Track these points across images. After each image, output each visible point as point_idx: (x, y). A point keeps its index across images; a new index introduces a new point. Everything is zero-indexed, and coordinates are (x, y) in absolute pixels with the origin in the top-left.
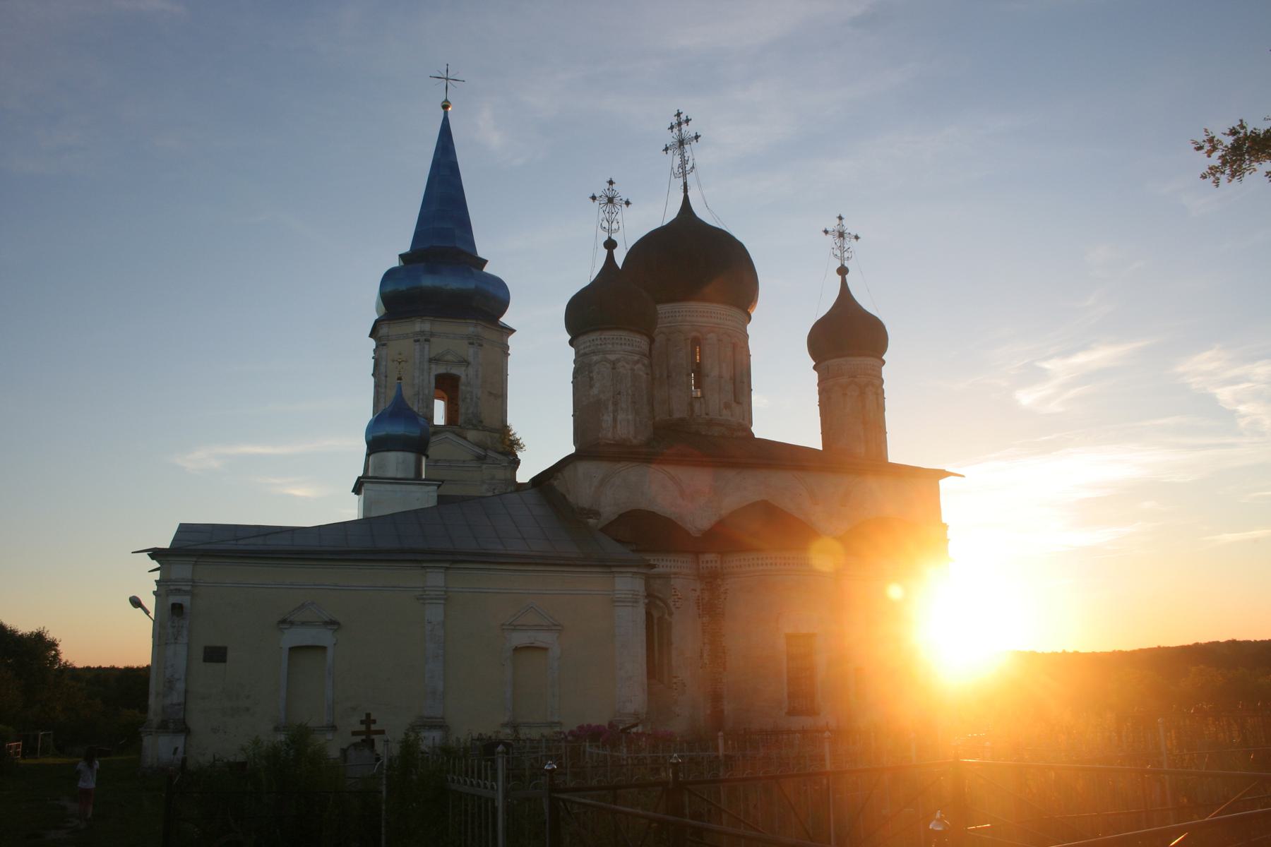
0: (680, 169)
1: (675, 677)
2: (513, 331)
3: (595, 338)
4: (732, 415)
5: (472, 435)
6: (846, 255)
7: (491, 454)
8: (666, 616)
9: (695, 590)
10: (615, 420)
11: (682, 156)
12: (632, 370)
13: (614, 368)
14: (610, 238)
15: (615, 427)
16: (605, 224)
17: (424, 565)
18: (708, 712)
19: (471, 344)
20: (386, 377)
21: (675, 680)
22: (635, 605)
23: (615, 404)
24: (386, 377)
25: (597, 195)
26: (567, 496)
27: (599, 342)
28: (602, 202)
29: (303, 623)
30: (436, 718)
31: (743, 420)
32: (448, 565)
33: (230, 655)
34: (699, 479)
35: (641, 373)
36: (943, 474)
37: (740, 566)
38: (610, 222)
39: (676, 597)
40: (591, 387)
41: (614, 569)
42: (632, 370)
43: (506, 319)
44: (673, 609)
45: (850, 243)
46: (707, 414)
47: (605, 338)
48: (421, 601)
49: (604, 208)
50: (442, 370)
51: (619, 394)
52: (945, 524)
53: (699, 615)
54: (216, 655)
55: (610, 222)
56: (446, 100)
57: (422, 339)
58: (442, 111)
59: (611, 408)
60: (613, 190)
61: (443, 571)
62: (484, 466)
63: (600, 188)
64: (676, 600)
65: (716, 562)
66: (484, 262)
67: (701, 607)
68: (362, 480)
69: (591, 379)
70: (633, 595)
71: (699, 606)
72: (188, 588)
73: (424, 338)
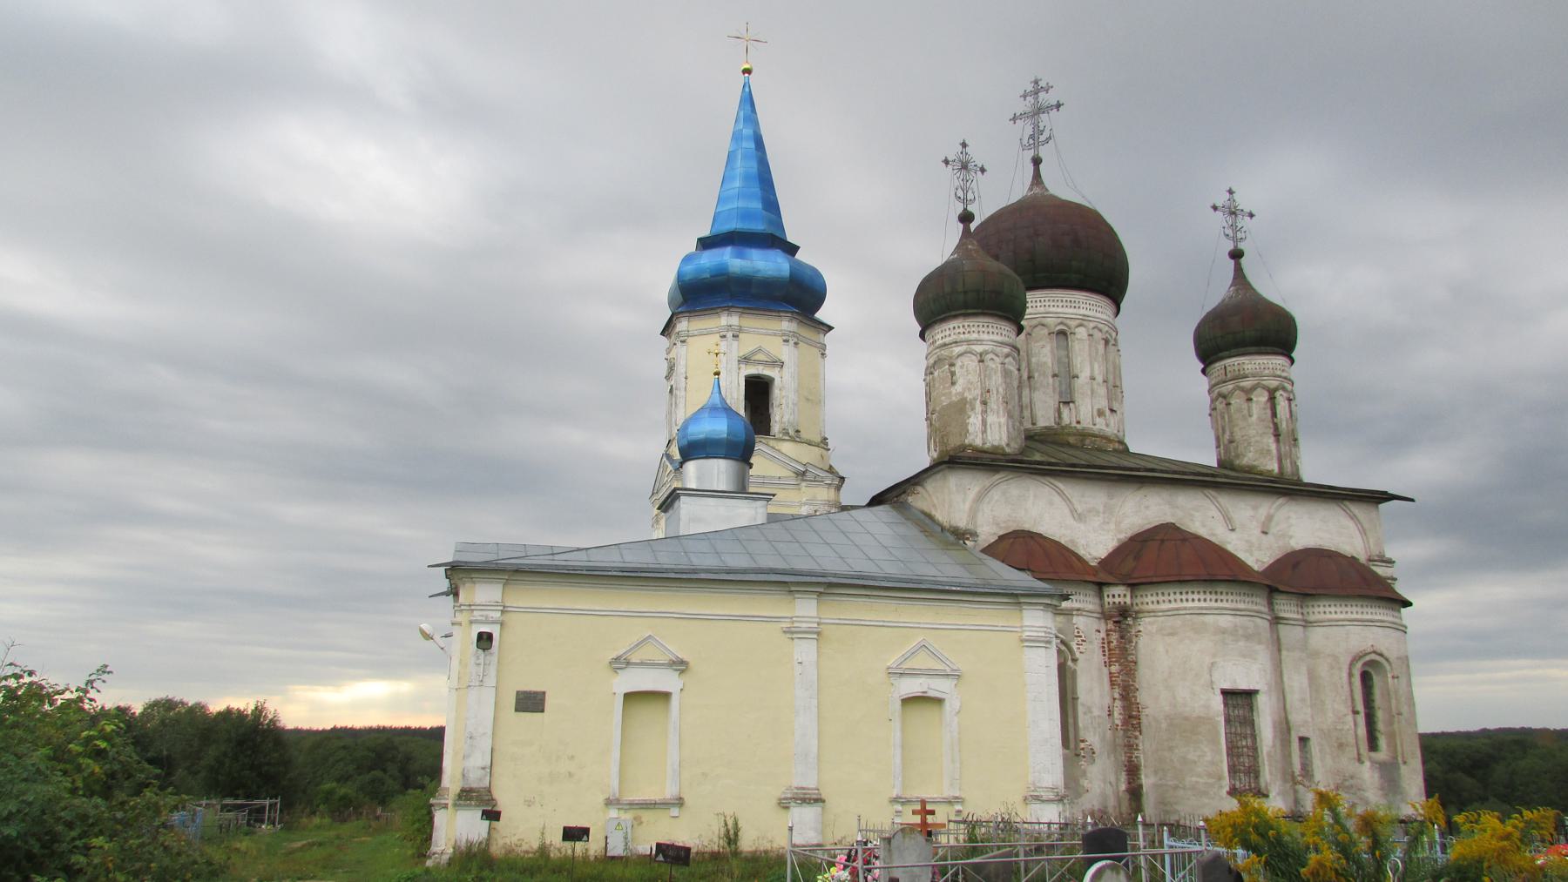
1: (1083, 741)
2: (831, 328)
3: (956, 325)
4: (1107, 425)
5: (787, 448)
6: (1239, 235)
8: (1070, 663)
9: (1099, 632)
10: (984, 422)
13: (981, 361)
14: (965, 209)
15: (984, 432)
17: (793, 589)
18: (1123, 787)
21: (1082, 745)
22: (1048, 646)
23: (984, 403)
25: (949, 159)
26: (933, 513)
27: (961, 330)
28: (955, 167)
29: (642, 664)
30: (808, 789)
32: (822, 590)
33: (549, 703)
34: (1090, 497)
35: (1012, 368)
37: (1158, 602)
38: (965, 191)
39: (1079, 639)
40: (953, 383)
41: (1022, 600)
43: (819, 315)
44: (1078, 655)
45: (1243, 222)
46: (1078, 422)
48: (789, 636)
49: (958, 174)
50: (753, 370)
51: (988, 391)
53: (1105, 662)
54: (531, 702)
55: (965, 191)
60: (966, 154)
61: (815, 596)
62: (804, 484)
63: (953, 152)
64: (1081, 643)
65: (1125, 596)
67: (1107, 653)
68: (678, 492)
69: (953, 374)
70: (1045, 632)
71: (1104, 651)
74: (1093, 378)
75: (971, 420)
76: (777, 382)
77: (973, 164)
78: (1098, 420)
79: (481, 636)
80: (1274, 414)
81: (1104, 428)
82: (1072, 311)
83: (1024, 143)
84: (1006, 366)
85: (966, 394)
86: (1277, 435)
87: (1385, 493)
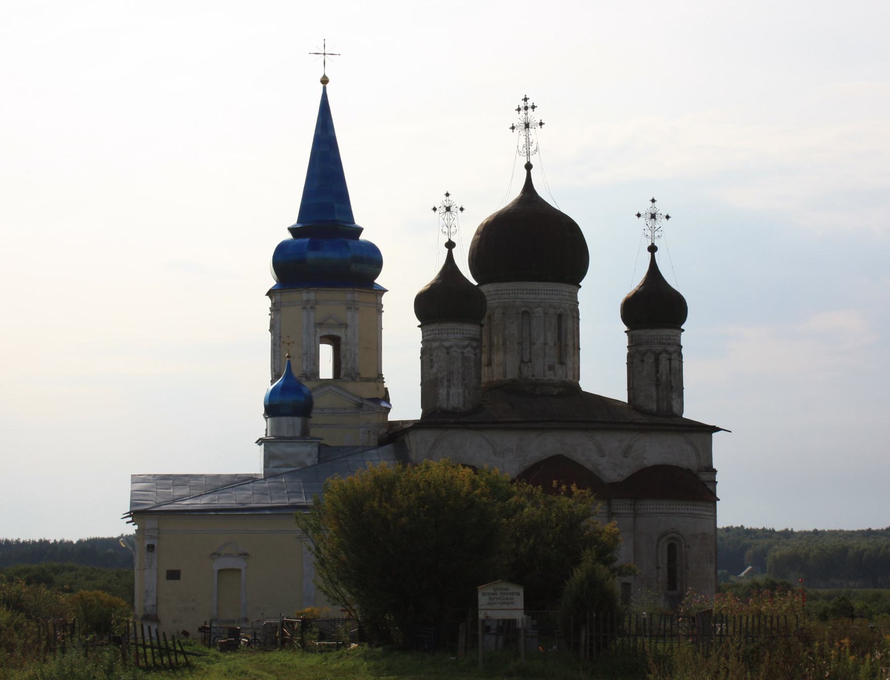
0: (524, 149)
2: (386, 291)
4: (555, 375)
6: (657, 234)
7: (365, 402)
11: (527, 138)
12: (463, 353)
13: (448, 353)
14: (450, 240)
15: (448, 399)
16: (446, 229)
19: (350, 308)
20: (280, 337)
23: (449, 381)
24: (280, 337)
27: (437, 332)
29: (226, 555)
31: (566, 377)
33: (182, 575)
36: (716, 429)
40: (432, 367)
42: (463, 353)
43: (379, 281)
45: (661, 222)
47: (441, 329)
51: (452, 373)
52: (715, 469)
54: (173, 575)
56: (325, 76)
57: (309, 306)
58: (322, 86)
59: (445, 384)
60: (449, 200)
66: (359, 230)
69: (432, 360)
72: (156, 535)
73: (309, 306)
74: (545, 344)
75: (441, 391)
76: (343, 339)
77: (455, 207)
78: (548, 373)
79: (148, 546)
80: (657, 371)
81: (553, 378)
82: (534, 296)
83: (520, 151)
84: (465, 354)
85: (439, 375)
86: (657, 385)
87: (714, 427)
